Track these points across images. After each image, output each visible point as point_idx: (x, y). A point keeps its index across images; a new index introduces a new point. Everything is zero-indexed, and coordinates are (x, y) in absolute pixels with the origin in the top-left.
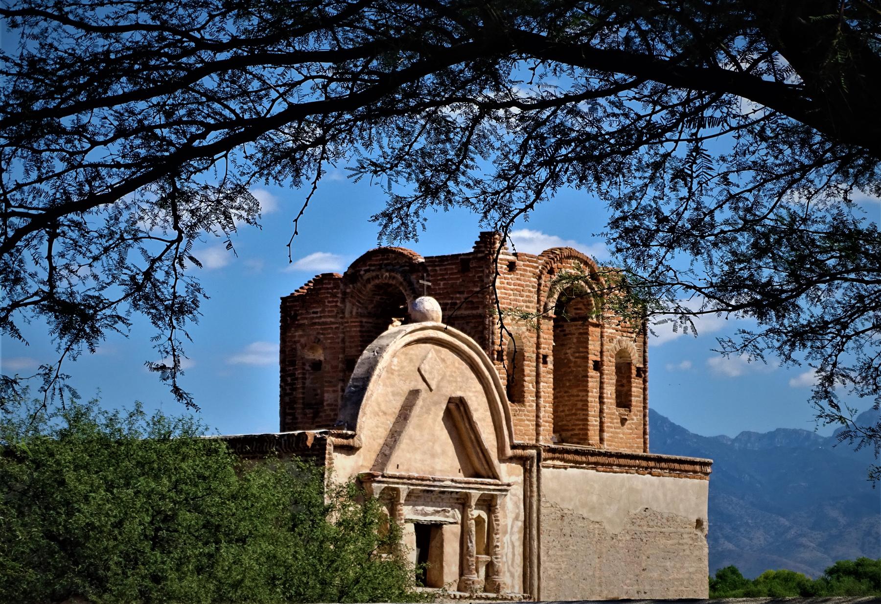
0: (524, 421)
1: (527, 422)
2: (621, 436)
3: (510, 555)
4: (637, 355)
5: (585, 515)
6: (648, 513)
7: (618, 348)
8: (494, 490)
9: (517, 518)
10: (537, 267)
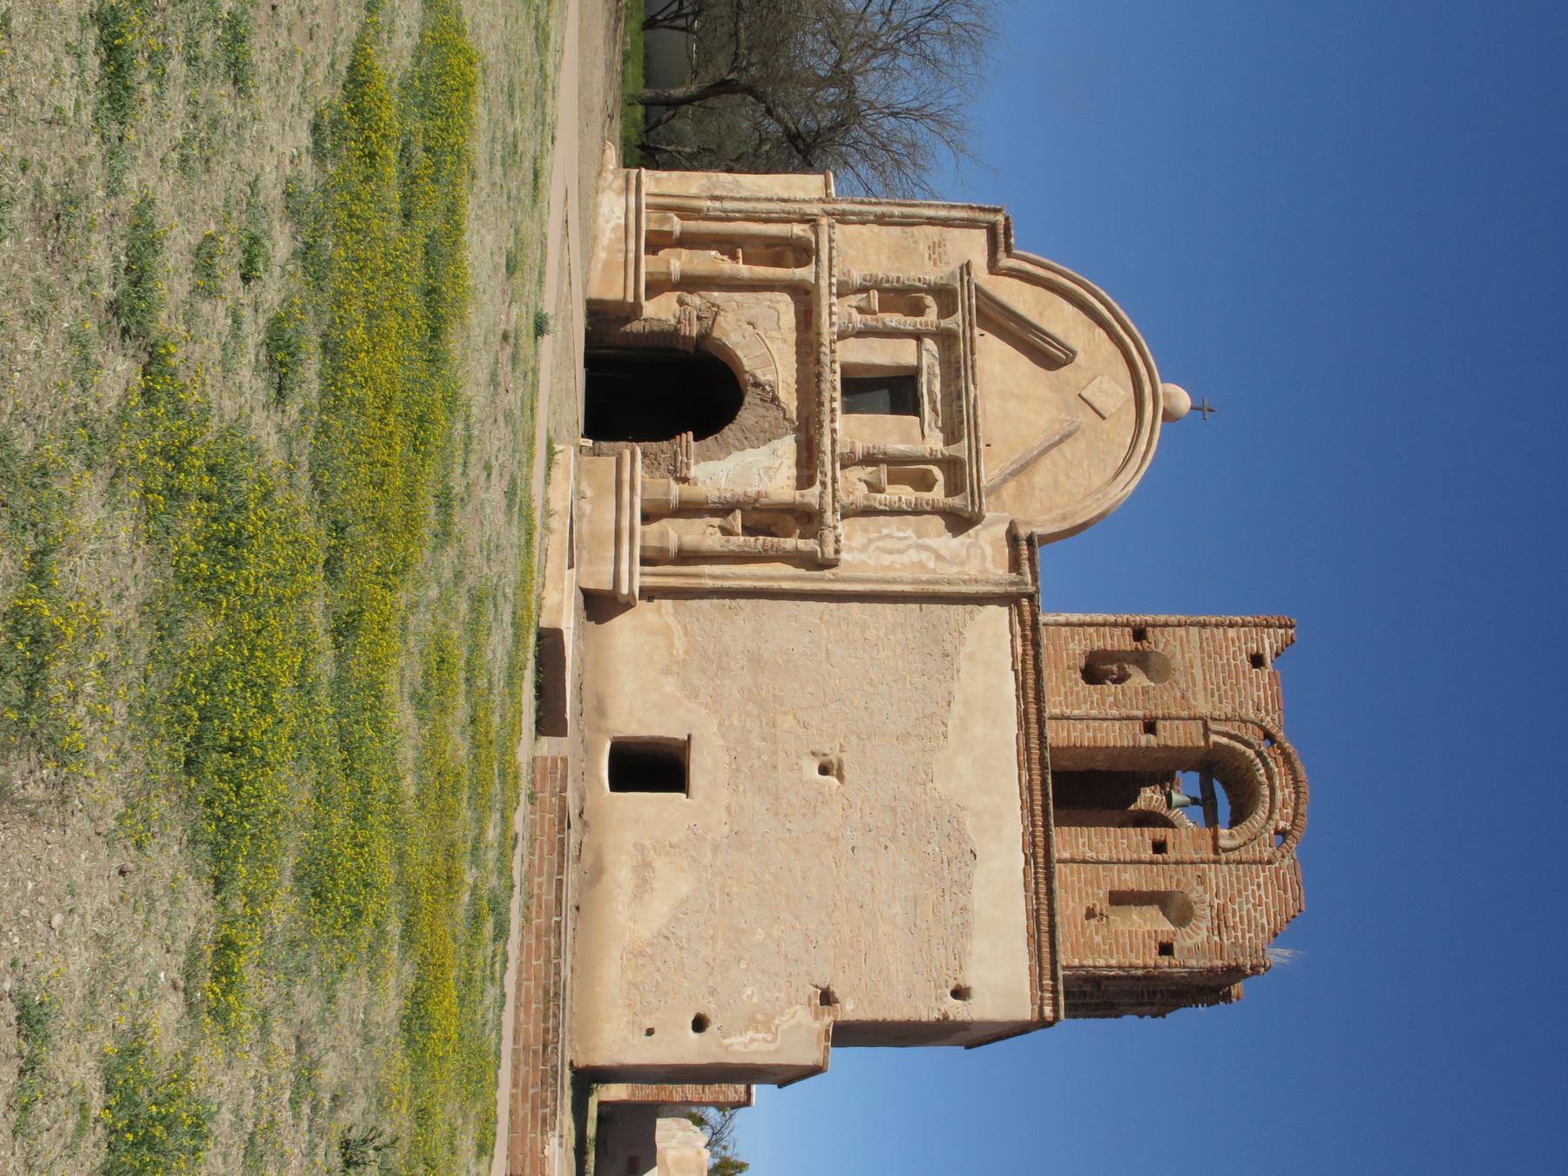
0: (1064, 685)
1: (1063, 690)
2: (1071, 904)
3: (889, 544)
4: (1189, 942)
5: (955, 707)
6: (968, 856)
7: (1193, 896)
8: (971, 482)
9: (939, 557)
10: (1267, 711)
